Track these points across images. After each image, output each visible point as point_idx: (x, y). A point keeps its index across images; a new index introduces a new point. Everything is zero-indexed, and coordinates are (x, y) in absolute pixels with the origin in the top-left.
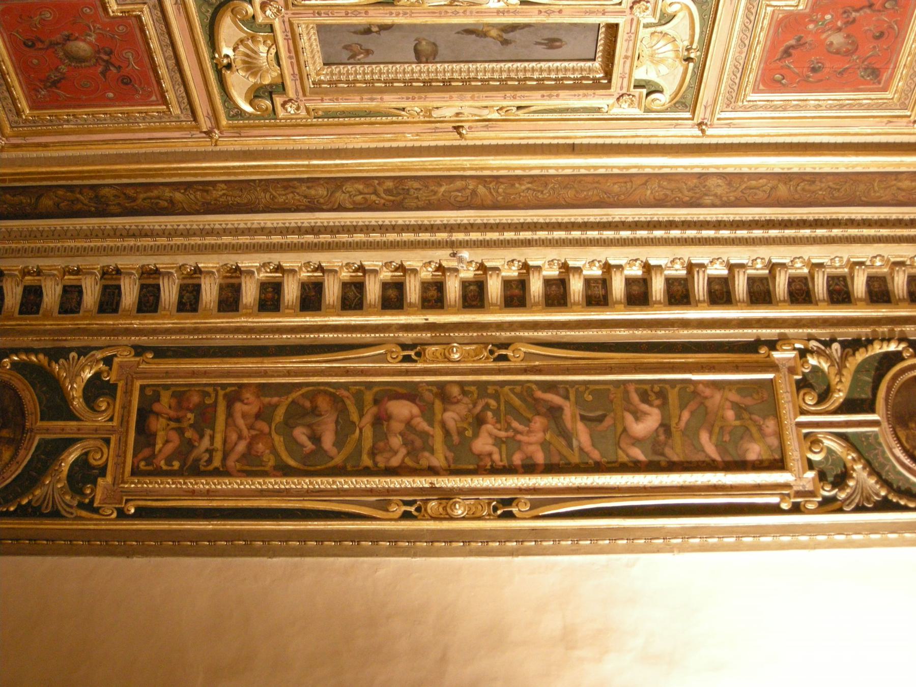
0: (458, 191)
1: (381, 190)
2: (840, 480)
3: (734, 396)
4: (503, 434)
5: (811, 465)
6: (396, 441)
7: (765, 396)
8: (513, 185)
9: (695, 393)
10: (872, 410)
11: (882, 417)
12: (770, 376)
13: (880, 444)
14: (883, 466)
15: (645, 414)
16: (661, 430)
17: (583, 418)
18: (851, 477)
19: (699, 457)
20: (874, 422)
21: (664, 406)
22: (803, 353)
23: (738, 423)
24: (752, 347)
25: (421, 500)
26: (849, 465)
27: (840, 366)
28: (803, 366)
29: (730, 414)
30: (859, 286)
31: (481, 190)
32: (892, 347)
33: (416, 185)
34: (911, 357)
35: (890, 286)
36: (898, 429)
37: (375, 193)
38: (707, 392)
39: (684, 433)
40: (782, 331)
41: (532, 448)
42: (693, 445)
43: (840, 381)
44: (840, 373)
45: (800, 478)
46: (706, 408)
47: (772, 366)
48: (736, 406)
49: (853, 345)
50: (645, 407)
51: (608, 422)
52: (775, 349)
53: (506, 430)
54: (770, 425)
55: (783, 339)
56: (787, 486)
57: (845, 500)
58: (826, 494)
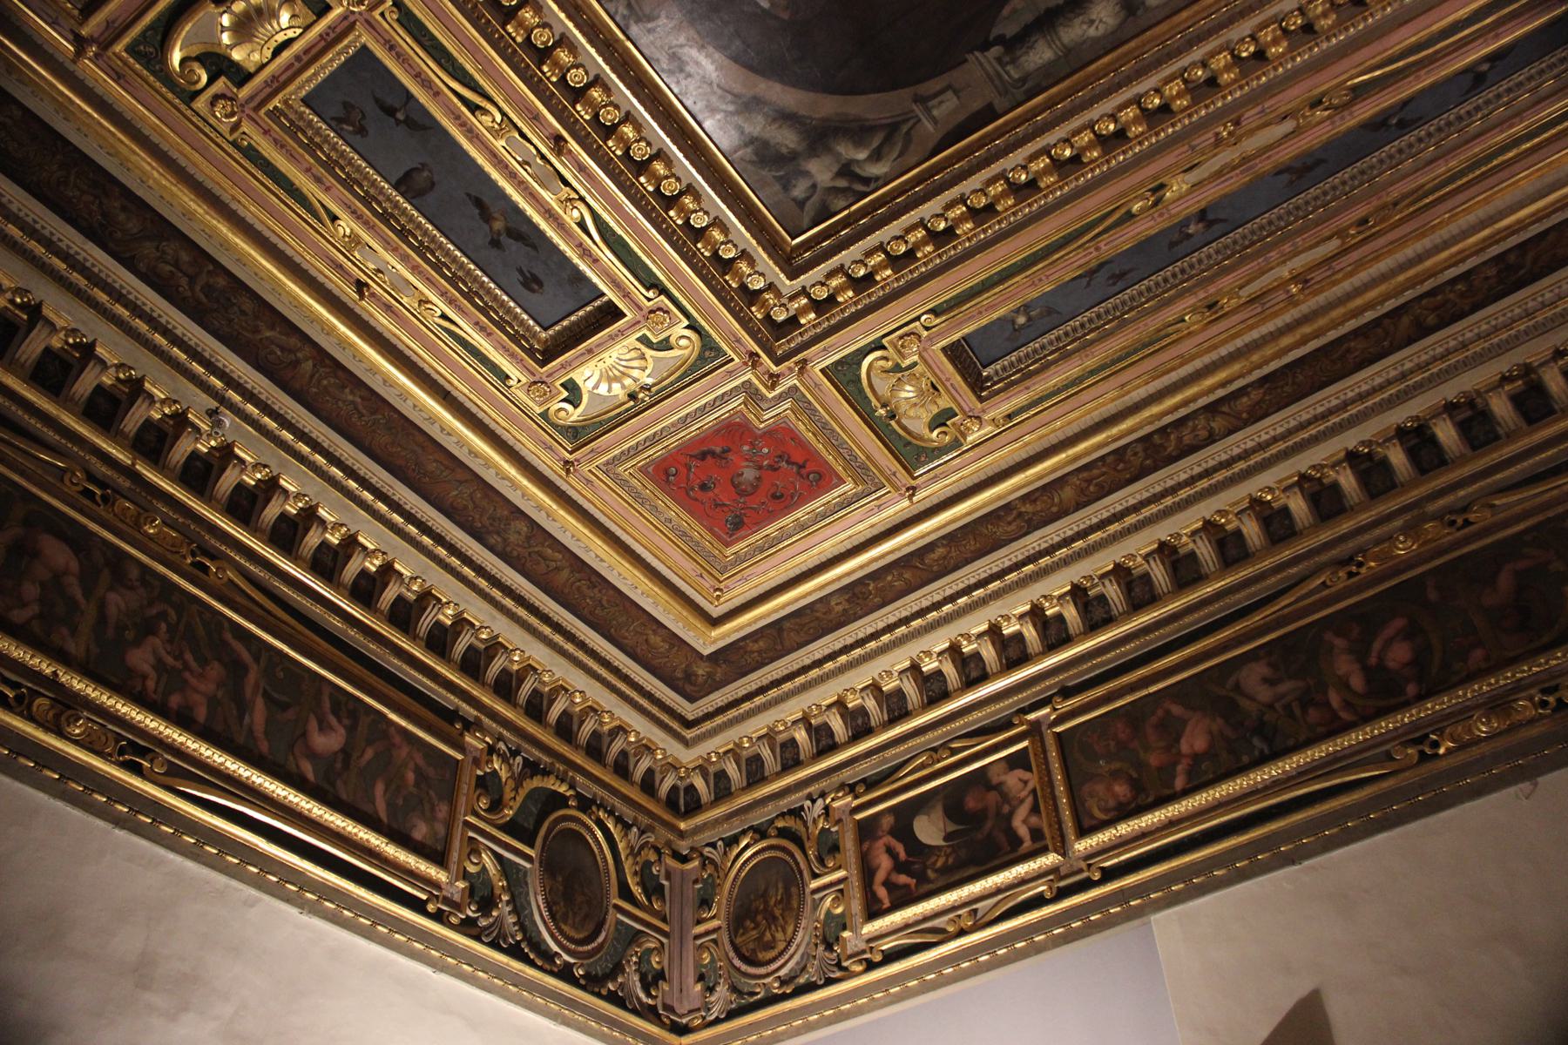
0: (282, 349)
1: (203, 280)
2: (487, 903)
3: (419, 759)
4: (169, 660)
5: (465, 875)
6: (31, 590)
8: (344, 387)
10: (532, 846)
12: (460, 757)
15: (331, 728)
16: (340, 757)
17: (266, 694)
20: (526, 858)
21: (351, 730)
22: (491, 750)
24: (452, 716)
25: (28, 688)
26: (497, 892)
27: (519, 781)
29: (411, 776)
31: (308, 366)
32: (562, 789)
33: (248, 306)
37: (192, 279)
38: (397, 739)
41: (197, 697)
44: (516, 789)
47: (461, 747)
48: (418, 771)
50: (333, 720)
51: (290, 714)
53: (176, 658)
54: (443, 810)
56: (436, 885)
57: (486, 928)
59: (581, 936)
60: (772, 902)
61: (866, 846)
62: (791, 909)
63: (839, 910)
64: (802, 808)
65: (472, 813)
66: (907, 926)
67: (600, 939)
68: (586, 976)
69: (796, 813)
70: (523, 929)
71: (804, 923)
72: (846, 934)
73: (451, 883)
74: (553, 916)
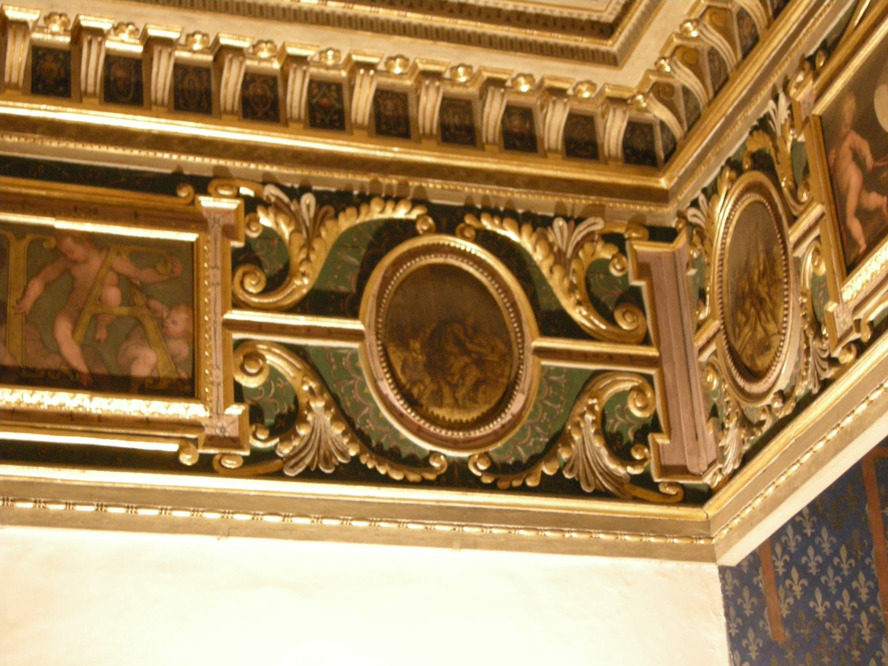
2: (284, 426)
3: (124, 265)
5: (239, 394)
7: (178, 269)
9: (57, 253)
10: (353, 314)
11: (368, 327)
12: (190, 237)
13: (359, 371)
14: (359, 407)
18: (305, 421)
19: (50, 363)
20: (351, 333)
22: (251, 205)
23: (124, 311)
26: (303, 400)
27: (312, 235)
28: (248, 226)
29: (113, 295)
30: (362, 102)
32: (401, 213)
34: (429, 232)
35: (412, 110)
36: (391, 349)
38: (79, 252)
39: (29, 318)
40: (222, 162)
42: (42, 341)
43: (308, 259)
44: (308, 245)
45: (217, 414)
46: (73, 279)
47: (195, 220)
49: (337, 201)
52: (206, 193)
54: (179, 320)
55: (222, 177)
56: (194, 425)
57: (289, 458)
58: (259, 445)
59: (474, 415)
67: (515, 406)
68: (493, 469)
73: (217, 414)
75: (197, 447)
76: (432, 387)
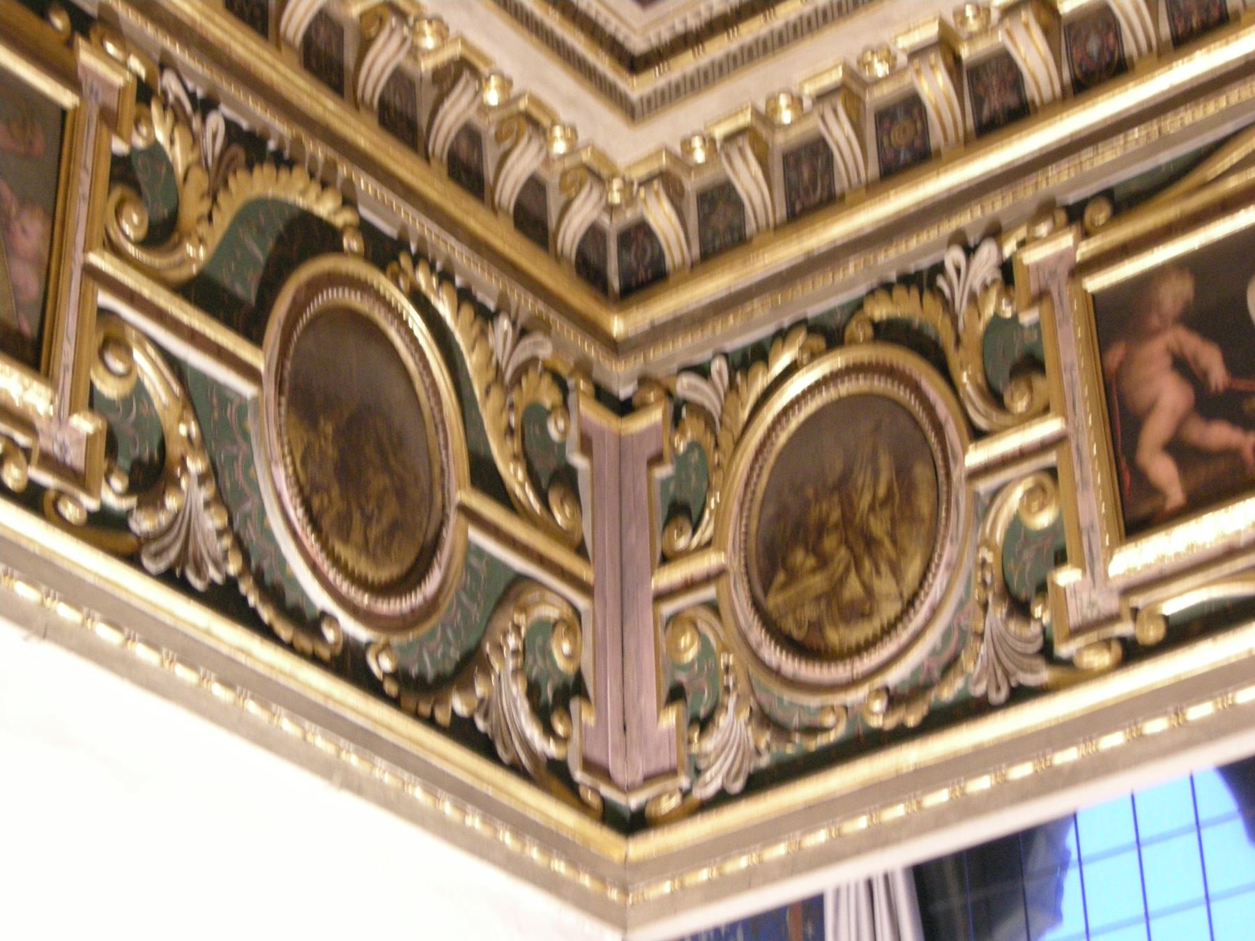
2: (151, 478)
5: (94, 402)
7: (39, 144)
10: (256, 339)
11: (268, 368)
12: (67, 98)
14: (242, 497)
22: (145, 92)
26: (174, 450)
32: (325, 207)
47: (68, 75)
49: (248, 147)
57: (148, 539)
59: (383, 574)
60: (865, 502)
61: (1116, 354)
62: (914, 519)
63: (1043, 519)
64: (939, 268)
65: (106, 252)
66: (1231, 552)
67: (431, 585)
68: (399, 675)
69: (924, 281)
70: (240, 544)
71: (948, 552)
72: (1066, 577)
73: (60, 419)
74: (314, 520)
75: (28, 461)
76: (339, 505)
